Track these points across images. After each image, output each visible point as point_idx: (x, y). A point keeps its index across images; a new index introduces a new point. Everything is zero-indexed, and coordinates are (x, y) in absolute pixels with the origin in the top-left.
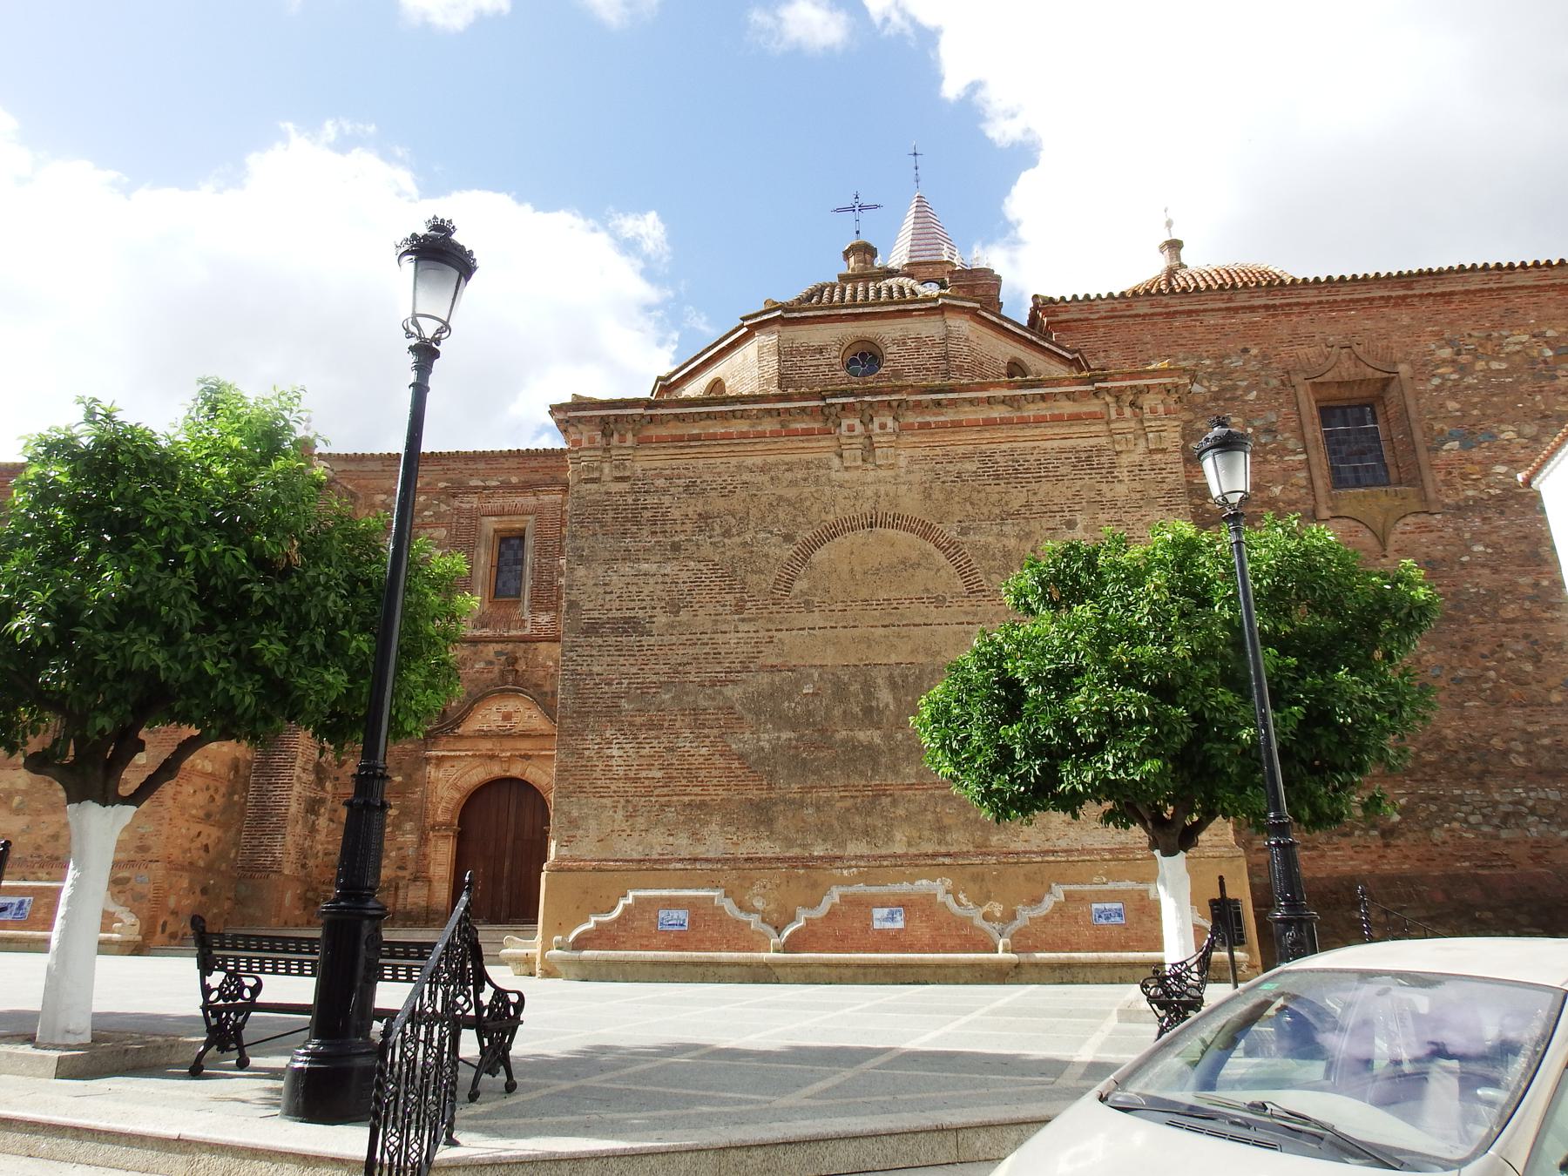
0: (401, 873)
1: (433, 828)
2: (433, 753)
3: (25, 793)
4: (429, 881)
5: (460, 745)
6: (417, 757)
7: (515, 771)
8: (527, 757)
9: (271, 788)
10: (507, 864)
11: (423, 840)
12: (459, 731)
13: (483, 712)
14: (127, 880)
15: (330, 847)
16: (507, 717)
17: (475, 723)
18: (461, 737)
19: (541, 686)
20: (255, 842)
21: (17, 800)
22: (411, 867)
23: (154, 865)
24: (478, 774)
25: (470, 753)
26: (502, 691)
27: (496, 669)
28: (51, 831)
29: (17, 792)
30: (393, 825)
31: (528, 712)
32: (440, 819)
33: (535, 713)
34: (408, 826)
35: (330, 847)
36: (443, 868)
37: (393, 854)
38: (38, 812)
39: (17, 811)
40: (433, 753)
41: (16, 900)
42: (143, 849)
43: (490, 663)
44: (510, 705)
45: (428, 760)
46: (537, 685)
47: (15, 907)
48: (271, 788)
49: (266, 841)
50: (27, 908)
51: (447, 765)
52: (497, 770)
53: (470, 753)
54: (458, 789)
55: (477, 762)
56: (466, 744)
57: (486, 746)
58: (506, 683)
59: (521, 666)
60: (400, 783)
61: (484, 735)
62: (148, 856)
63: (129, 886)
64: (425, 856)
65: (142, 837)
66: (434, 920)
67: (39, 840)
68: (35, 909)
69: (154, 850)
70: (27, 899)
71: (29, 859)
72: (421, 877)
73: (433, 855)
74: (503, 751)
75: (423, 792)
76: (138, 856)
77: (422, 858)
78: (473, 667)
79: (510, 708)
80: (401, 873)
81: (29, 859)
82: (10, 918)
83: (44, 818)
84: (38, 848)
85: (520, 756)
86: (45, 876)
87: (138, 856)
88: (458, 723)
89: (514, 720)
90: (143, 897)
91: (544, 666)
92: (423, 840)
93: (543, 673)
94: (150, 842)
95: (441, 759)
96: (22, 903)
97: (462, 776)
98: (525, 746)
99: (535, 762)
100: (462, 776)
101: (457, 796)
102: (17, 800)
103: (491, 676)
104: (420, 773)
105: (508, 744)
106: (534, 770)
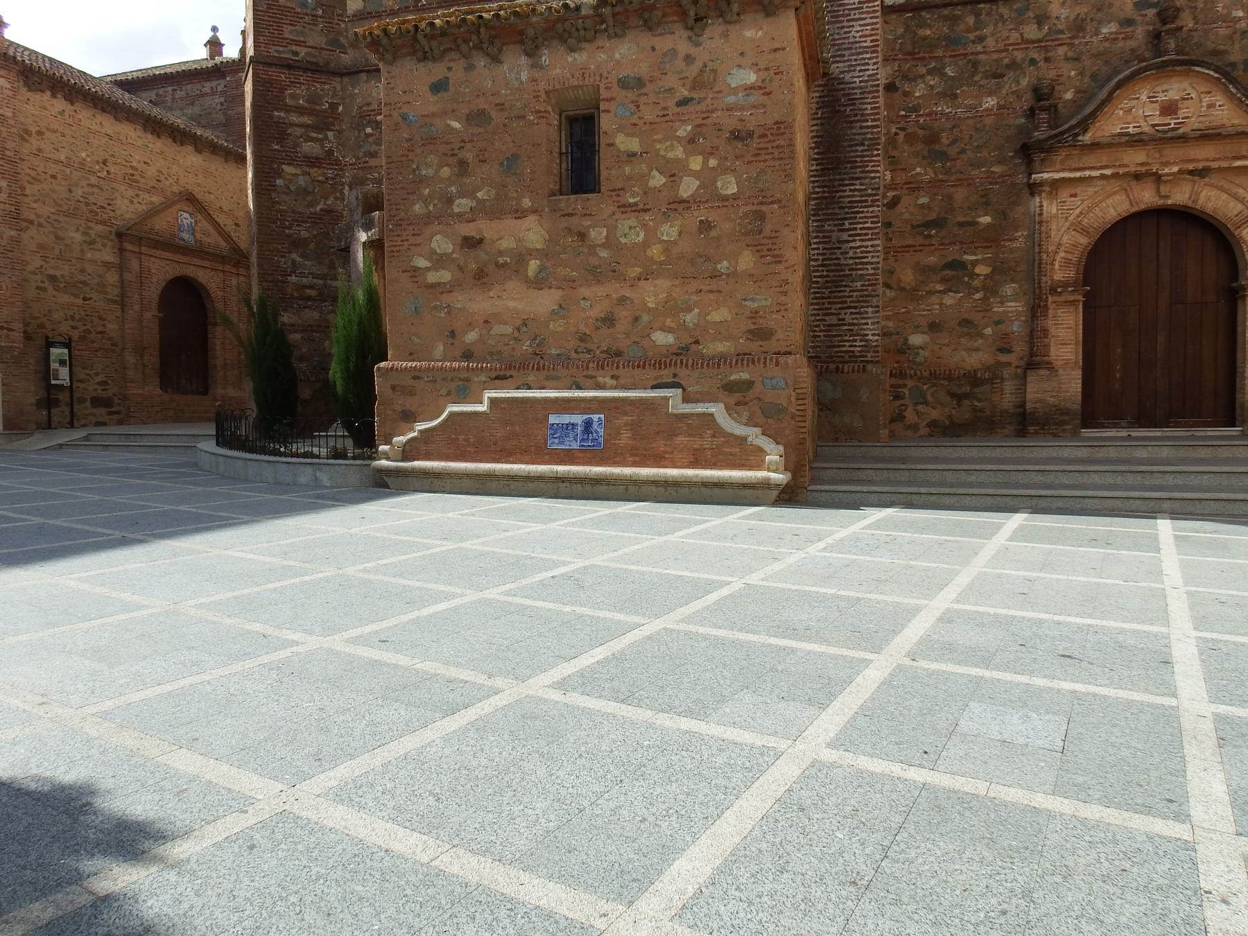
0: (1003, 358)
1: (1053, 291)
2: (1045, 176)
3: (543, 254)
4: (1050, 367)
5: (1089, 160)
6: (1013, 185)
7: (1179, 196)
8: (1202, 173)
9: (845, 236)
10: (1161, 339)
11: (1037, 310)
12: (1087, 138)
13: (1126, 104)
14: (749, 384)
15: (890, 324)
16: (1169, 109)
17: (1112, 124)
18: (1095, 146)
19: (1225, 52)
20: (833, 320)
21: (533, 265)
22: (1020, 348)
23: (790, 359)
24: (1115, 206)
25: (1108, 172)
26: (1164, 65)
27: (1140, 32)
28: (597, 312)
29: (532, 253)
30: (984, 288)
31: (1206, 100)
32: (1058, 276)
33: (1219, 99)
34: (1009, 289)
35: (890, 324)
36: (1069, 348)
37: (988, 331)
38: (572, 283)
39: (538, 283)
40: (1045, 176)
41: (578, 419)
42: (762, 334)
43: (1129, 22)
44: (1174, 89)
45: (1034, 188)
46: (1216, 53)
47: (579, 429)
48: (845, 236)
49: (848, 319)
50: (599, 430)
51: (1064, 194)
52: (1147, 197)
53: (1108, 172)
54: (1084, 231)
55: (1115, 185)
56: (1103, 157)
57: (1135, 158)
58: (1166, 52)
59: (1187, 21)
60: (988, 226)
61: (1136, 141)
62: (772, 345)
63: (751, 395)
64: (1045, 332)
65: (754, 315)
66: (1064, 423)
67: (582, 327)
68: (613, 433)
69: (780, 335)
70: (595, 417)
71: (574, 355)
72: (1035, 361)
73: (1053, 331)
74: (1167, 164)
75: (1031, 236)
76: (754, 346)
77: (1036, 335)
78: (1097, 33)
79: (1174, 95)
80: (1003, 358)
81: (574, 355)
82: (575, 446)
83: (584, 291)
84: (584, 338)
85: (1191, 172)
86: (608, 381)
87: (754, 346)
88: (1084, 125)
89: (1181, 113)
90: (783, 410)
91: (1228, 19)
92: (1037, 310)
93: (1224, 32)
94: (772, 321)
95: (1055, 185)
96: (588, 424)
97: (1090, 209)
98: (1204, 154)
99: (1214, 179)
100: (1090, 209)
101: (1084, 241)
102: (533, 265)
103: (1132, 43)
104: (1020, 209)
105: (1173, 152)
106: (1213, 193)
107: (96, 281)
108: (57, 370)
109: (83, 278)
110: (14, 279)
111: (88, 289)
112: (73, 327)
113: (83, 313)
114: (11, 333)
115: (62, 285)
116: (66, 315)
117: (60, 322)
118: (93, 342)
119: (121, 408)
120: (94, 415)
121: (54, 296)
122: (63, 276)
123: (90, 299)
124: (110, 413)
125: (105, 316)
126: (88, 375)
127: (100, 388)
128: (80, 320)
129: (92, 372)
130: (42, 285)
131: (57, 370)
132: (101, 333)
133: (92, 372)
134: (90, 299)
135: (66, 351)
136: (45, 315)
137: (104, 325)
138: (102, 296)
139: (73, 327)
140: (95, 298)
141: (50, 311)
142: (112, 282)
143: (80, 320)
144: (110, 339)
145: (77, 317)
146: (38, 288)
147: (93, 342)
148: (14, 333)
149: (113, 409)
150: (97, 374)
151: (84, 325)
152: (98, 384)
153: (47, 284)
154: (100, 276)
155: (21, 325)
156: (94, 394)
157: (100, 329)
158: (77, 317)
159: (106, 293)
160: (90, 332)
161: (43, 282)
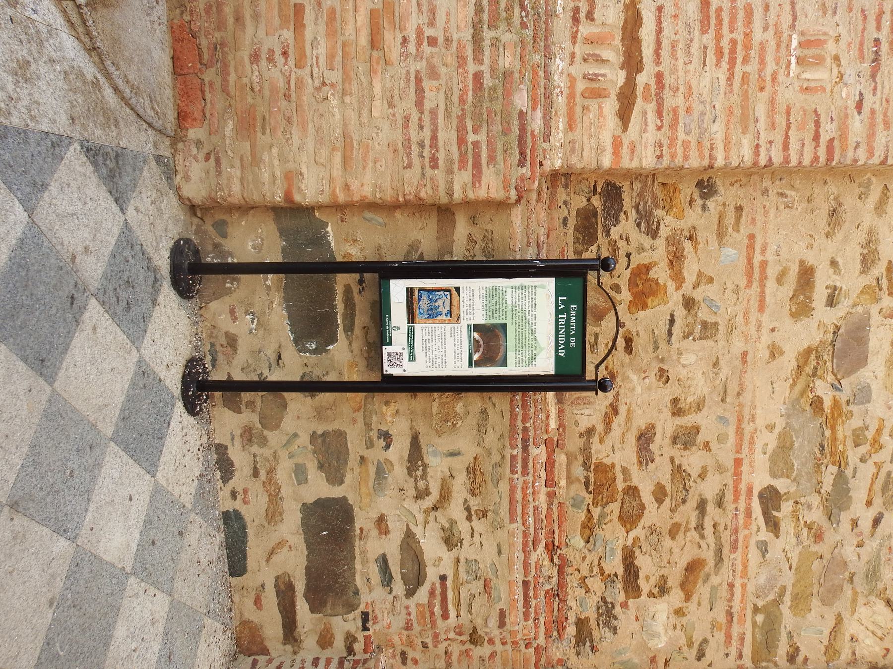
107: (849, 552)
108: (453, 315)
109: (859, 493)
110: (857, 125)
111: (816, 515)
112: (645, 438)
113: (709, 488)
114: (611, 105)
115: (822, 389)
116: (699, 407)
117: (663, 376)
118: (589, 529)
119: (310, 643)
120: (273, 515)
121: (775, 352)
122: (863, 395)
123: (773, 525)
124: (285, 592)
125: (702, 591)
126: (445, 496)
127: (391, 547)
128: (678, 471)
129: (456, 510)
130: (820, 294)
131: (453, 315)
132: (631, 572)
133: (456, 510)
134: (773, 525)
135: (545, 365)
136: (689, 304)
137: (663, 589)
138: (788, 579)
139: (645, 438)
140: (777, 547)
141: (708, 329)
142: (851, 627)
143: (678, 471)
144: (607, 611)
145: (693, 461)
146: (806, 275)
147: (589, 529)
148: (611, 121)
149: (302, 607)
150: (450, 540)
151: (660, 494)
152: (410, 543)
153: (831, 316)
154: (873, 574)
155: (647, 160)
156: (363, 520)
157: (643, 562)
158: (693, 461)
159: (800, 602)
160: (629, 520)
161: (831, 302)
